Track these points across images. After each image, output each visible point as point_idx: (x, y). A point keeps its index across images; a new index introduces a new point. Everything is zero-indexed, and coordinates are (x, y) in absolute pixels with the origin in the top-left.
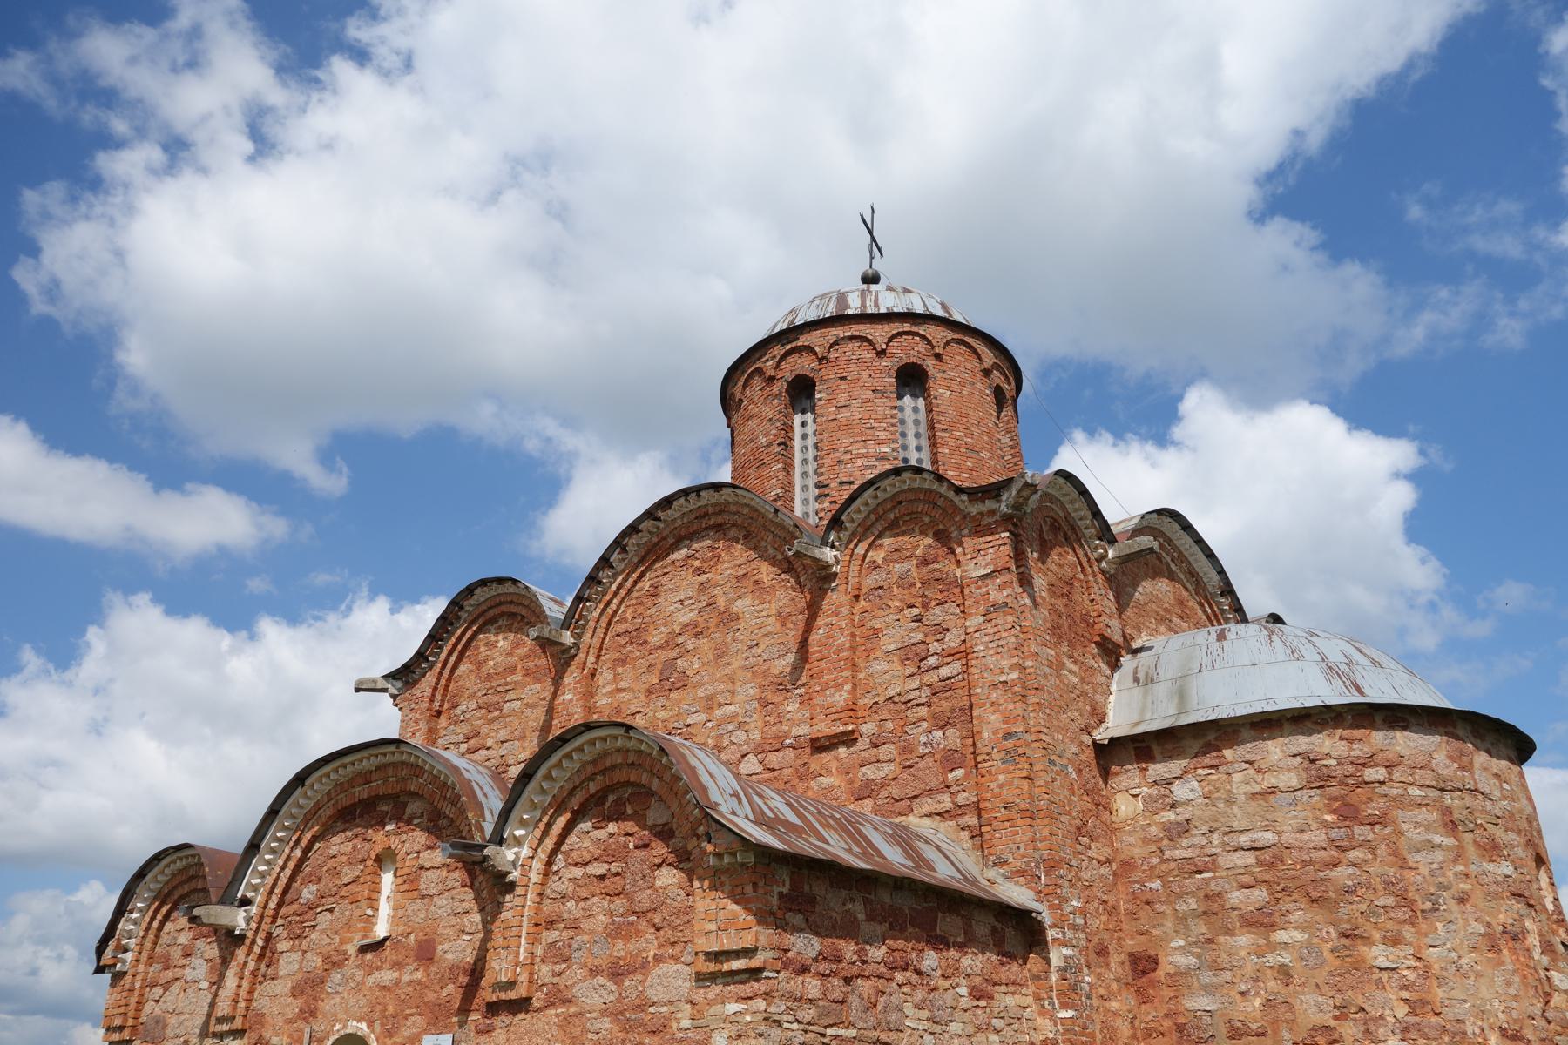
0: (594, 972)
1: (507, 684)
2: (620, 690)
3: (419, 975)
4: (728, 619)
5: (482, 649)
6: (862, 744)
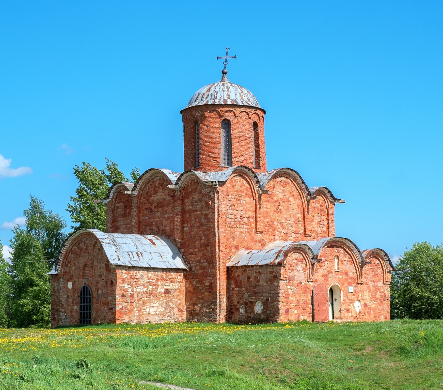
0: (371, 281)
1: (242, 195)
2: (268, 208)
3: (346, 277)
4: (289, 201)
5: (234, 182)
6: (311, 238)
